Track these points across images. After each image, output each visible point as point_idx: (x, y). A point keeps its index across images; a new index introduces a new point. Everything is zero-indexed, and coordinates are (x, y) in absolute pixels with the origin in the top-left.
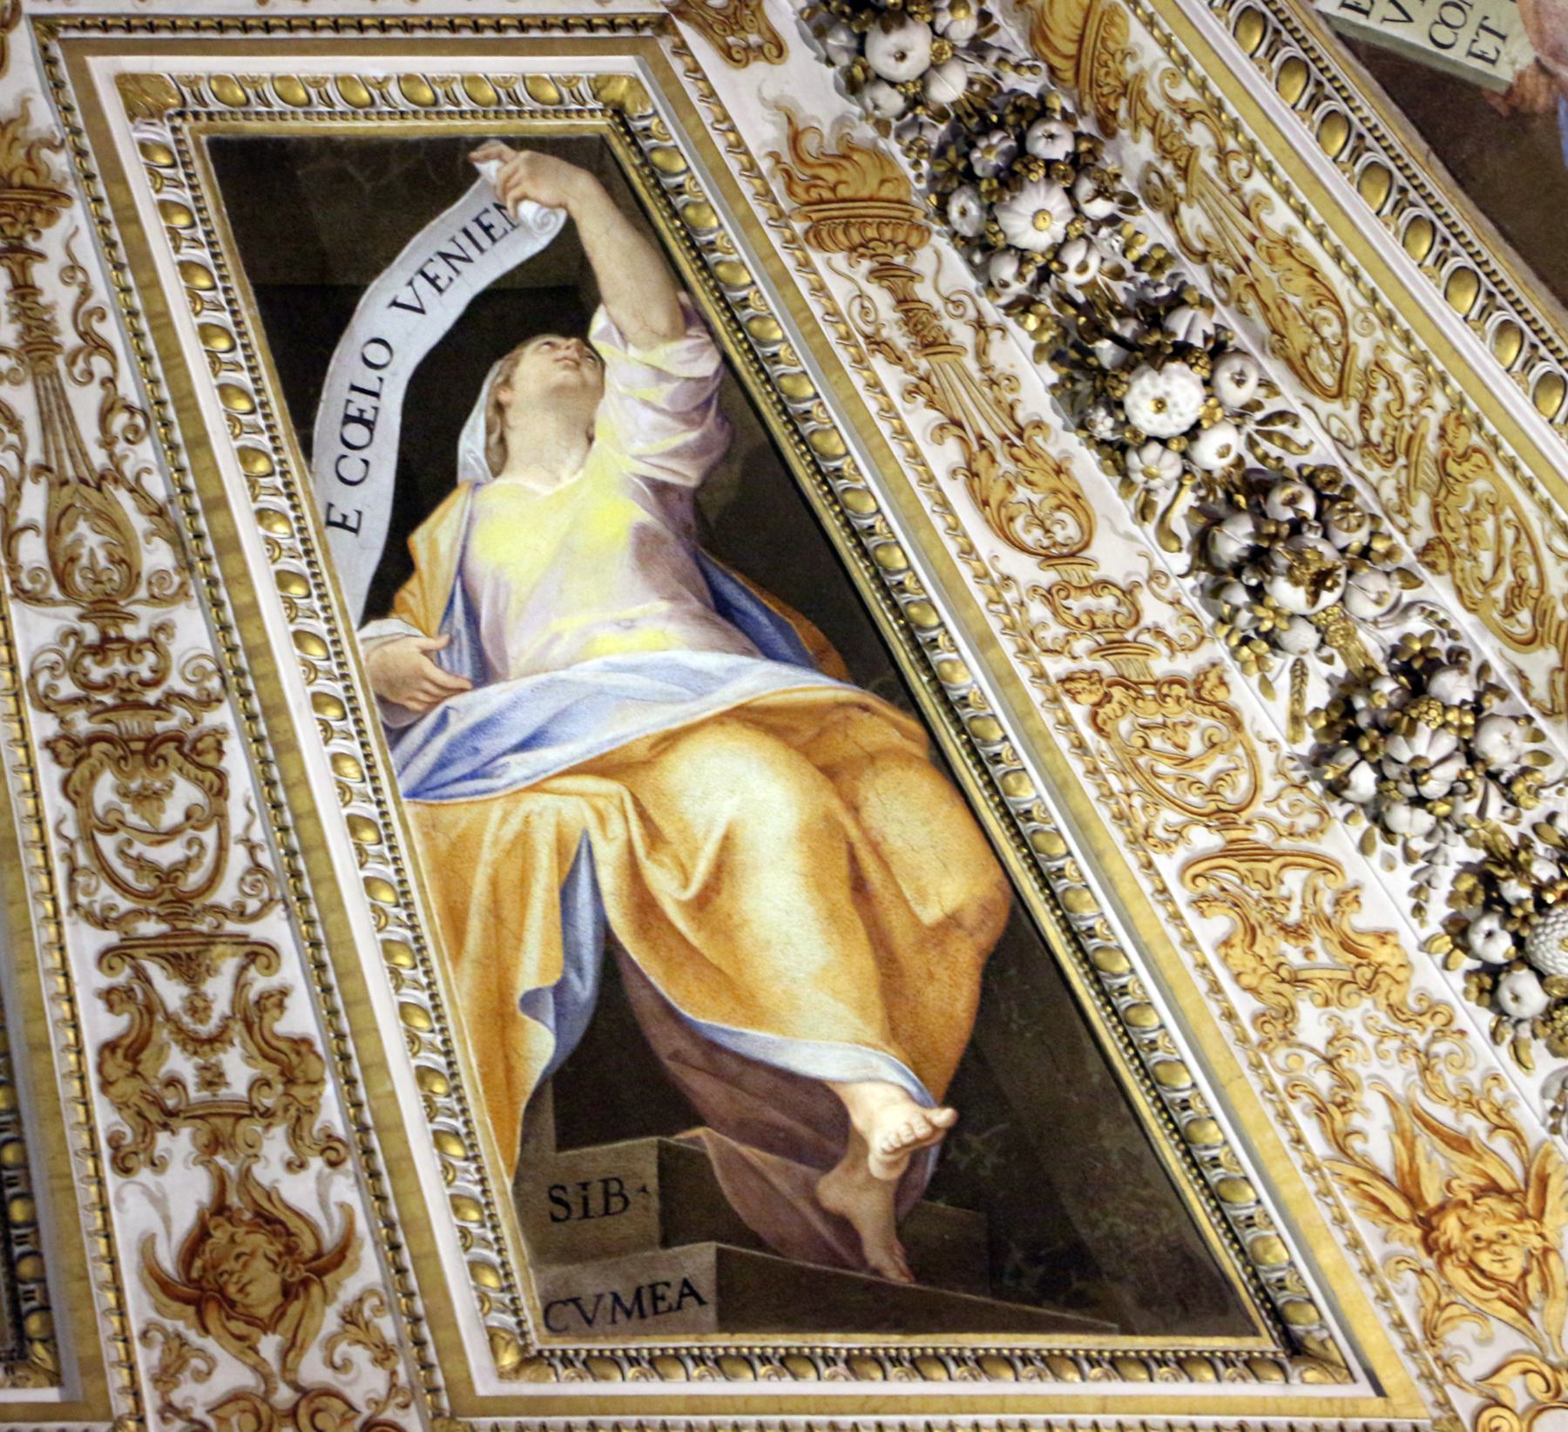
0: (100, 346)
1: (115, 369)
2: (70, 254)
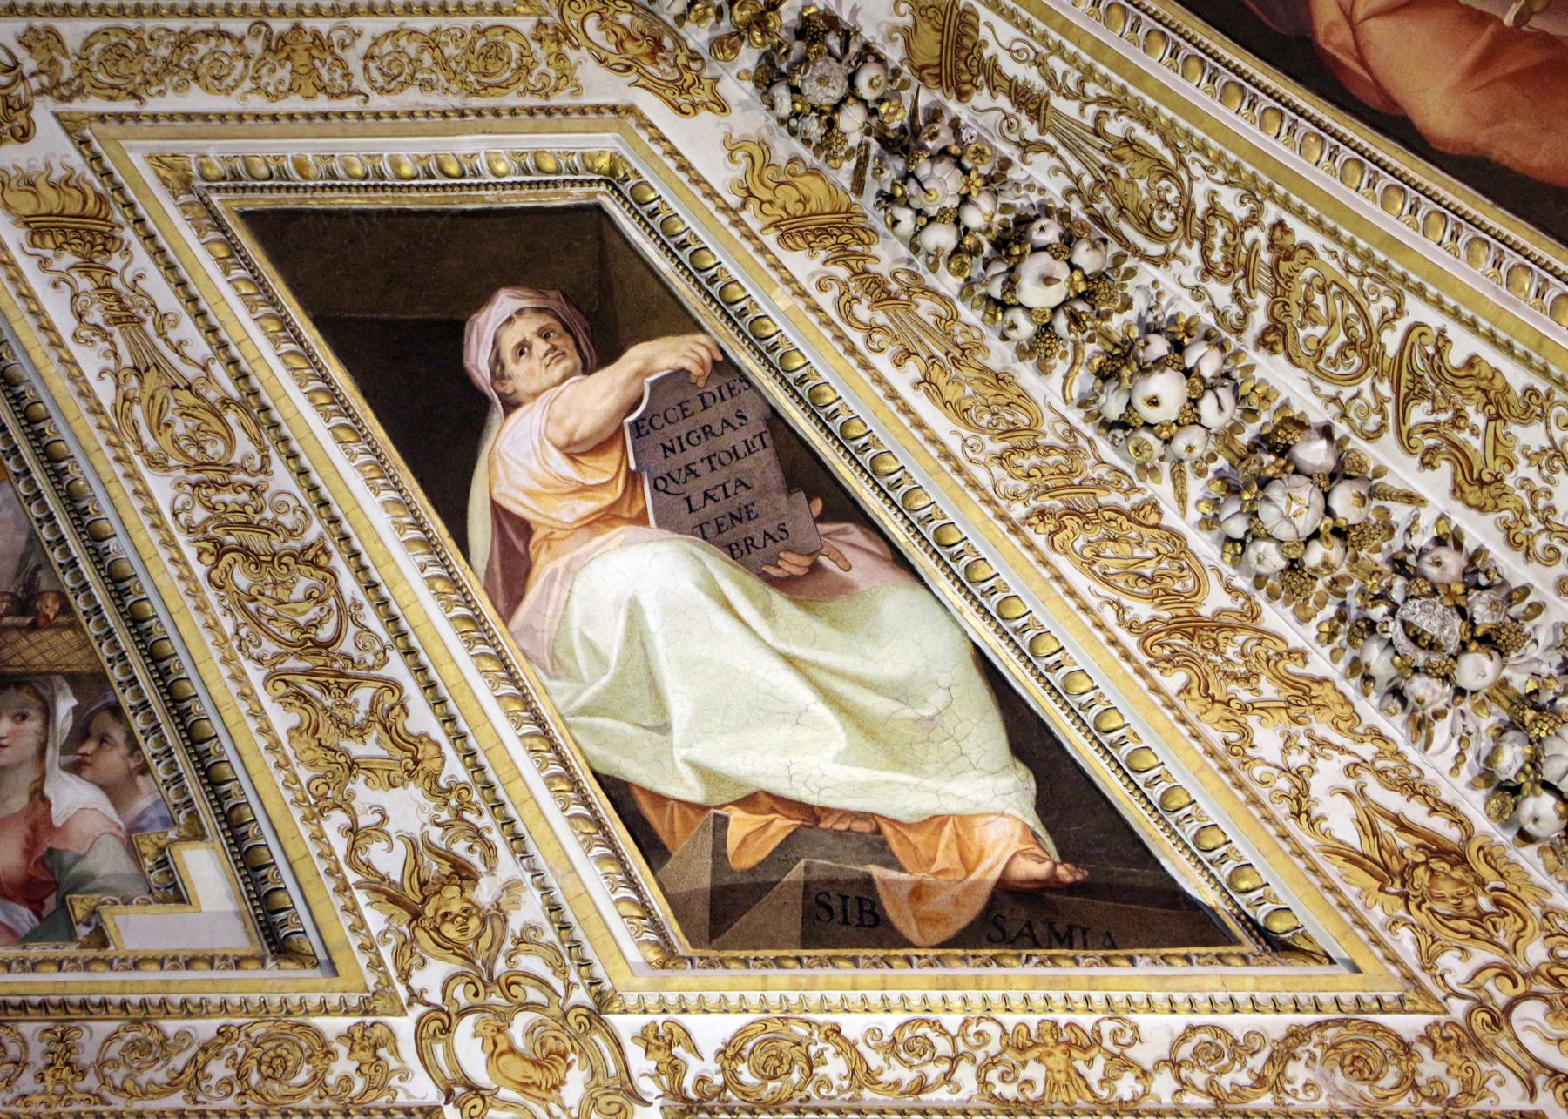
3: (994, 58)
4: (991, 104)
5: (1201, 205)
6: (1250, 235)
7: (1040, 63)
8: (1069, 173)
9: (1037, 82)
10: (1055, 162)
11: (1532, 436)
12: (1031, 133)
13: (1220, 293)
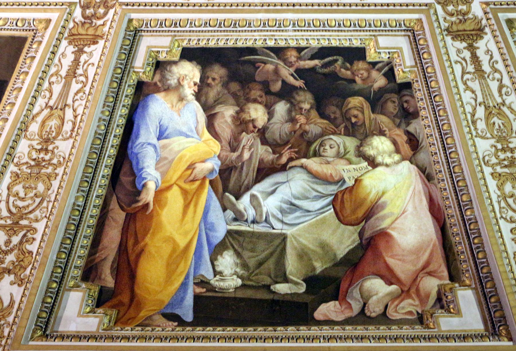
0: (496, 71)
1: (502, 76)
2: (487, 48)
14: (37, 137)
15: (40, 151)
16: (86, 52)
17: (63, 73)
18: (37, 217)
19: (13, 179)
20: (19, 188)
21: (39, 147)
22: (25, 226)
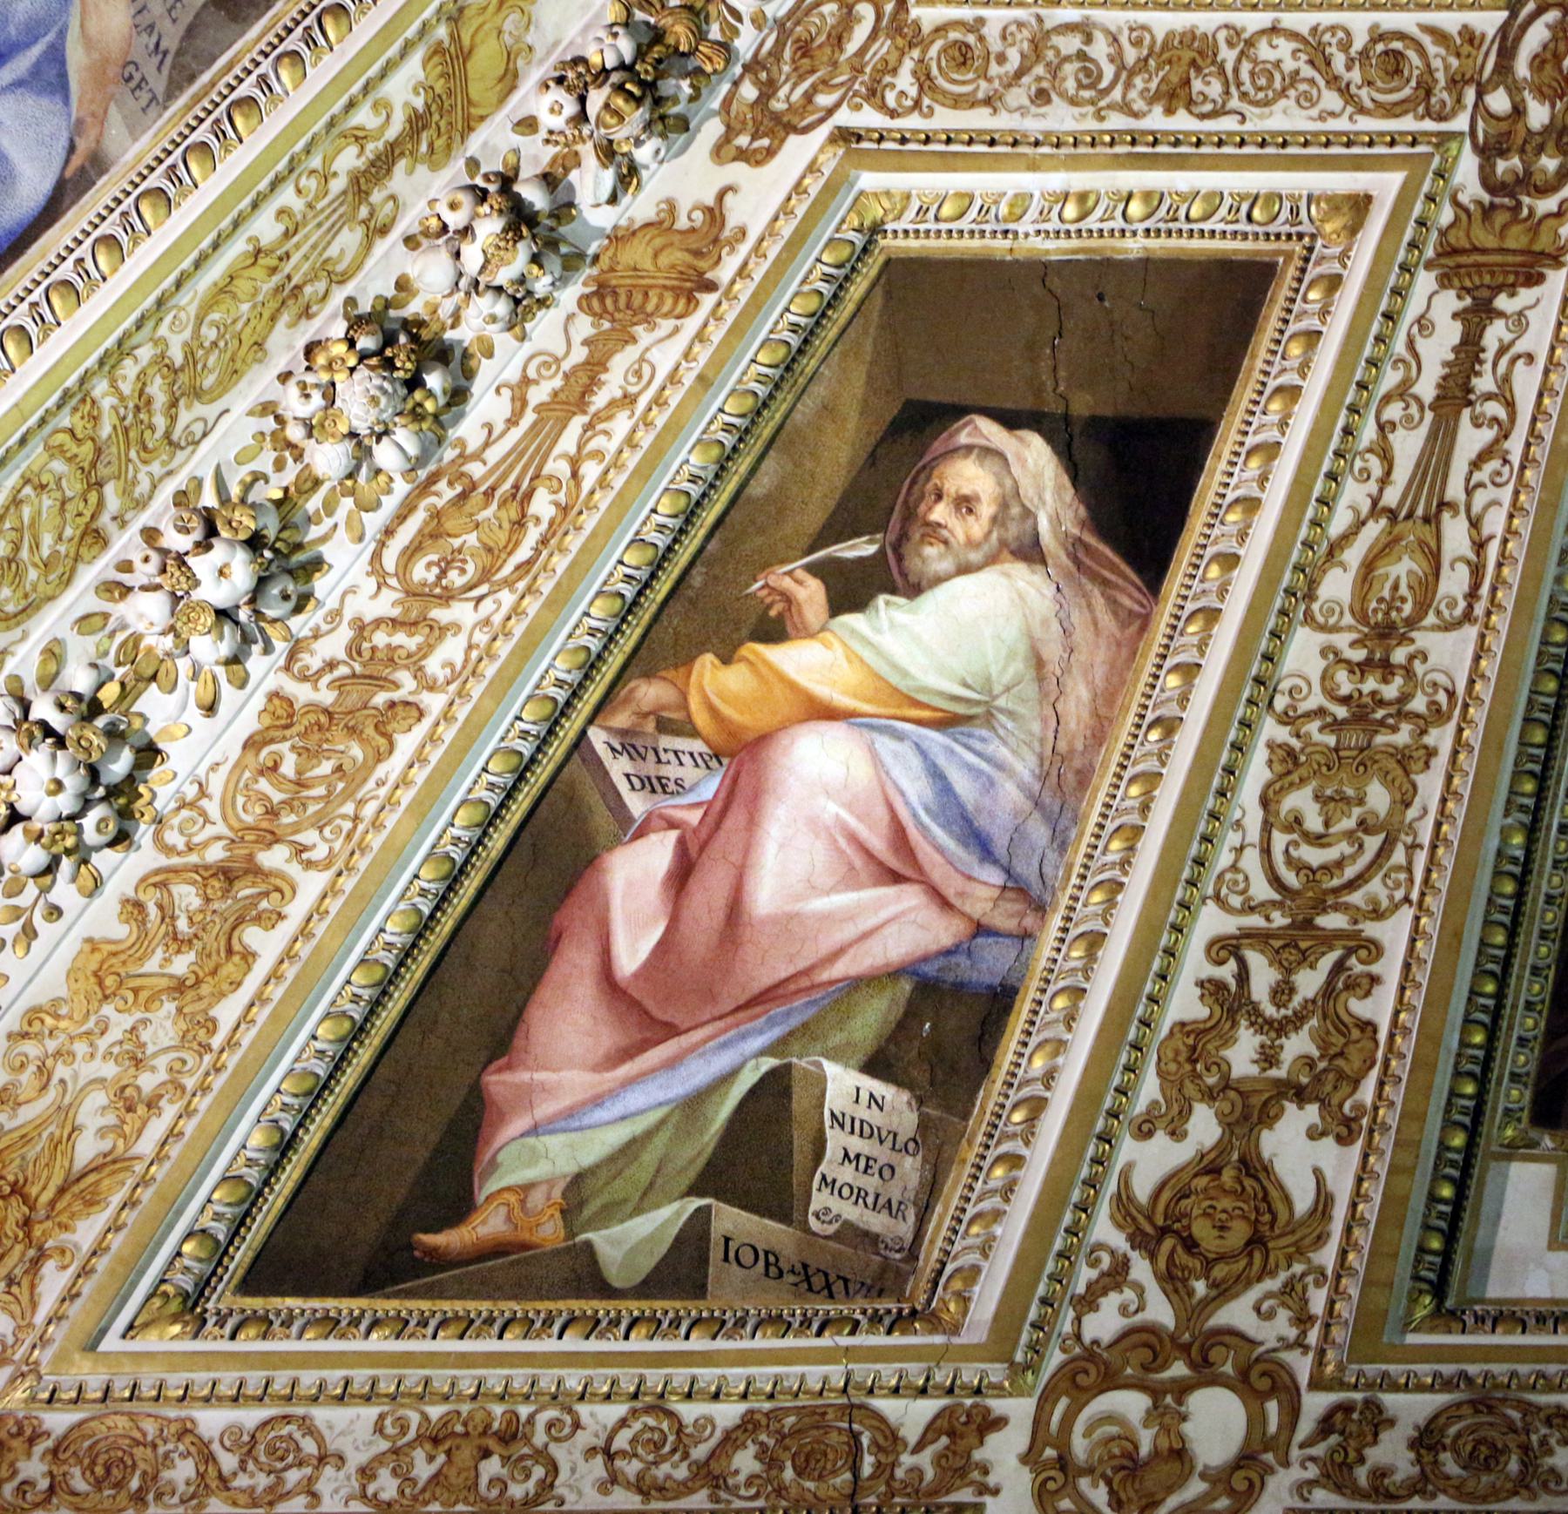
3: (633, 340)
4: (577, 339)
5: (440, 614)
6: (406, 679)
7: (629, 400)
8: (487, 445)
9: (599, 400)
10: (499, 427)
11: (163, 1027)
12: (538, 395)
13: (334, 645)
14: (1348, 619)
15: (1362, 668)
16: (1501, 314)
17: (1426, 388)
18: (1375, 902)
19: (1278, 768)
20: (1301, 801)
21: (1359, 655)
22: (1338, 935)
